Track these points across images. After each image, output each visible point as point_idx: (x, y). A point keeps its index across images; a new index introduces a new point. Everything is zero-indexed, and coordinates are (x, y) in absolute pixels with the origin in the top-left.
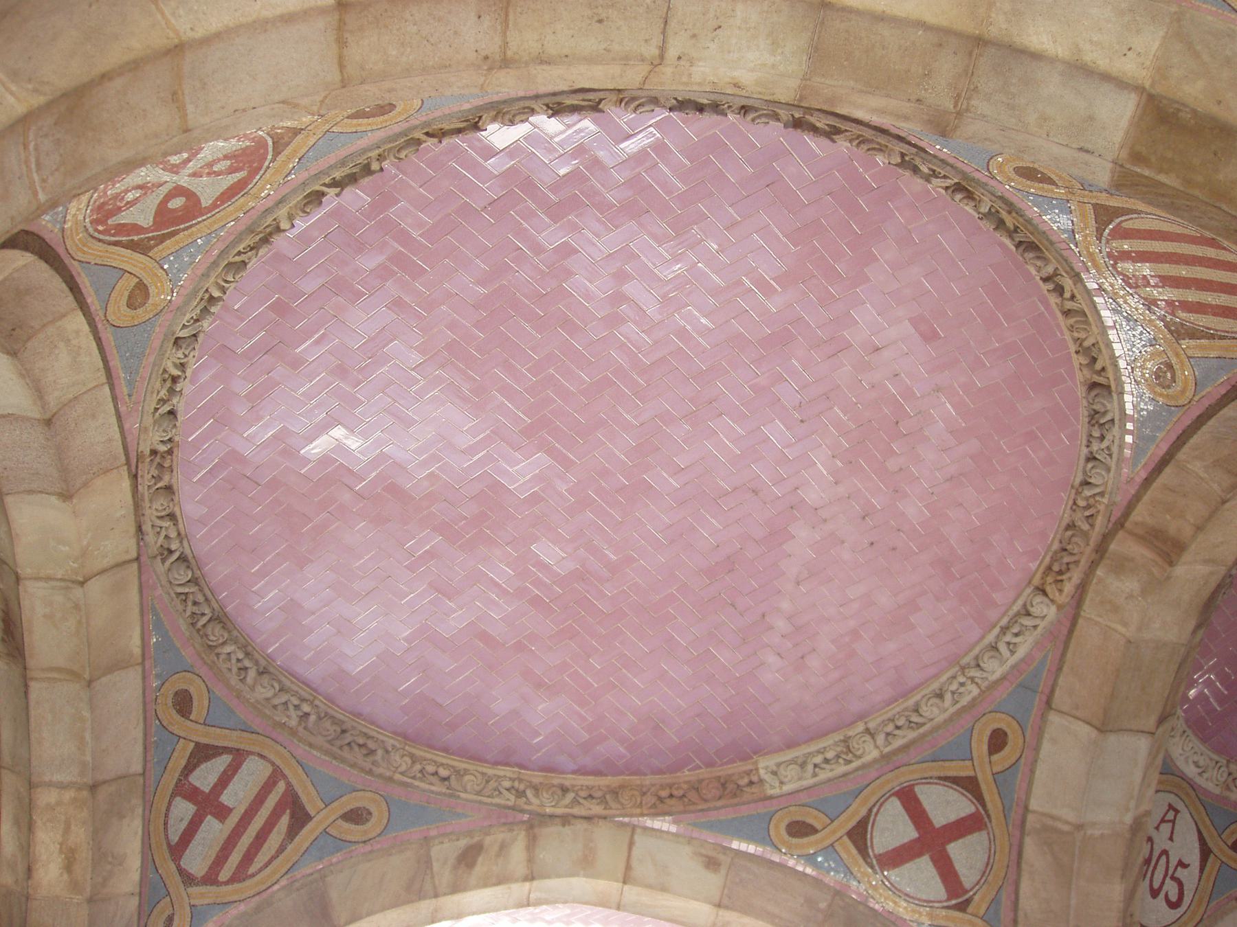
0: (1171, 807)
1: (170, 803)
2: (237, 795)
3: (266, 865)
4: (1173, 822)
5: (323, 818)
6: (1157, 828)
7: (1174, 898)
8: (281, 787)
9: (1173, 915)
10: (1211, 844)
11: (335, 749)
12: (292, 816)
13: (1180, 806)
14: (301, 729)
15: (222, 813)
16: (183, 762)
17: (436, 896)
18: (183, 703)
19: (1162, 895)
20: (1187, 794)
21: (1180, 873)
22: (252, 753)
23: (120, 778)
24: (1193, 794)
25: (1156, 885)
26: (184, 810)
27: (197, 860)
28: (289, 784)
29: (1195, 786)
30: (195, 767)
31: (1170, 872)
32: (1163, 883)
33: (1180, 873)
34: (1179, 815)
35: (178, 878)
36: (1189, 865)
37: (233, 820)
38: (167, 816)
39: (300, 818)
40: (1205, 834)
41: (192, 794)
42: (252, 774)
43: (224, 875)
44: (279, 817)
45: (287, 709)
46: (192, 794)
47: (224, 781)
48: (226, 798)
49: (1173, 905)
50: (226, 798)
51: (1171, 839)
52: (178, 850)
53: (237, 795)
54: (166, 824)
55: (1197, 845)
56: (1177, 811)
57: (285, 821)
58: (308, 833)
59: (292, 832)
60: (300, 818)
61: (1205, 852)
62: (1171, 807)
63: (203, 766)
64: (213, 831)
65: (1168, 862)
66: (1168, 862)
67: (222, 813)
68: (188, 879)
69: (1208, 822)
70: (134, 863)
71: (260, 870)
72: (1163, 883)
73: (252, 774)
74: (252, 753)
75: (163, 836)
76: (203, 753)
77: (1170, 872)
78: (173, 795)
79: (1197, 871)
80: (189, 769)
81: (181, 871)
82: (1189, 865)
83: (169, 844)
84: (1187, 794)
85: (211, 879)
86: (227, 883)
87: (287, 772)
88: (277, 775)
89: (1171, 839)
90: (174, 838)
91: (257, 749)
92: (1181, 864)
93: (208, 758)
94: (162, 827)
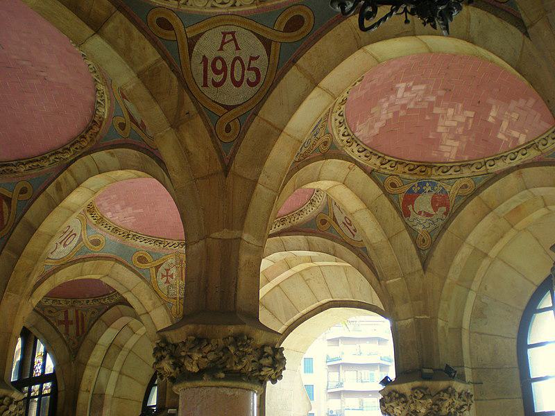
0: (224, 34)
4: (234, 39)
5: (15, 196)
6: (221, 49)
10: (269, 37)
12: (6, 201)
13: (233, 29)
17: (57, 206)
20: (232, 20)
21: (253, 64)
25: (238, 79)
31: (246, 67)
32: (243, 76)
33: (253, 64)
40: (261, 34)
49: (251, 84)
51: (238, 48)
55: (259, 42)
56: (233, 33)
58: (14, 203)
61: (267, 44)
62: (224, 34)
65: (242, 62)
66: (242, 62)
69: (260, 26)
72: (243, 76)
77: (246, 67)
79: (266, 57)
84: (232, 20)
89: (238, 48)
92: (252, 58)
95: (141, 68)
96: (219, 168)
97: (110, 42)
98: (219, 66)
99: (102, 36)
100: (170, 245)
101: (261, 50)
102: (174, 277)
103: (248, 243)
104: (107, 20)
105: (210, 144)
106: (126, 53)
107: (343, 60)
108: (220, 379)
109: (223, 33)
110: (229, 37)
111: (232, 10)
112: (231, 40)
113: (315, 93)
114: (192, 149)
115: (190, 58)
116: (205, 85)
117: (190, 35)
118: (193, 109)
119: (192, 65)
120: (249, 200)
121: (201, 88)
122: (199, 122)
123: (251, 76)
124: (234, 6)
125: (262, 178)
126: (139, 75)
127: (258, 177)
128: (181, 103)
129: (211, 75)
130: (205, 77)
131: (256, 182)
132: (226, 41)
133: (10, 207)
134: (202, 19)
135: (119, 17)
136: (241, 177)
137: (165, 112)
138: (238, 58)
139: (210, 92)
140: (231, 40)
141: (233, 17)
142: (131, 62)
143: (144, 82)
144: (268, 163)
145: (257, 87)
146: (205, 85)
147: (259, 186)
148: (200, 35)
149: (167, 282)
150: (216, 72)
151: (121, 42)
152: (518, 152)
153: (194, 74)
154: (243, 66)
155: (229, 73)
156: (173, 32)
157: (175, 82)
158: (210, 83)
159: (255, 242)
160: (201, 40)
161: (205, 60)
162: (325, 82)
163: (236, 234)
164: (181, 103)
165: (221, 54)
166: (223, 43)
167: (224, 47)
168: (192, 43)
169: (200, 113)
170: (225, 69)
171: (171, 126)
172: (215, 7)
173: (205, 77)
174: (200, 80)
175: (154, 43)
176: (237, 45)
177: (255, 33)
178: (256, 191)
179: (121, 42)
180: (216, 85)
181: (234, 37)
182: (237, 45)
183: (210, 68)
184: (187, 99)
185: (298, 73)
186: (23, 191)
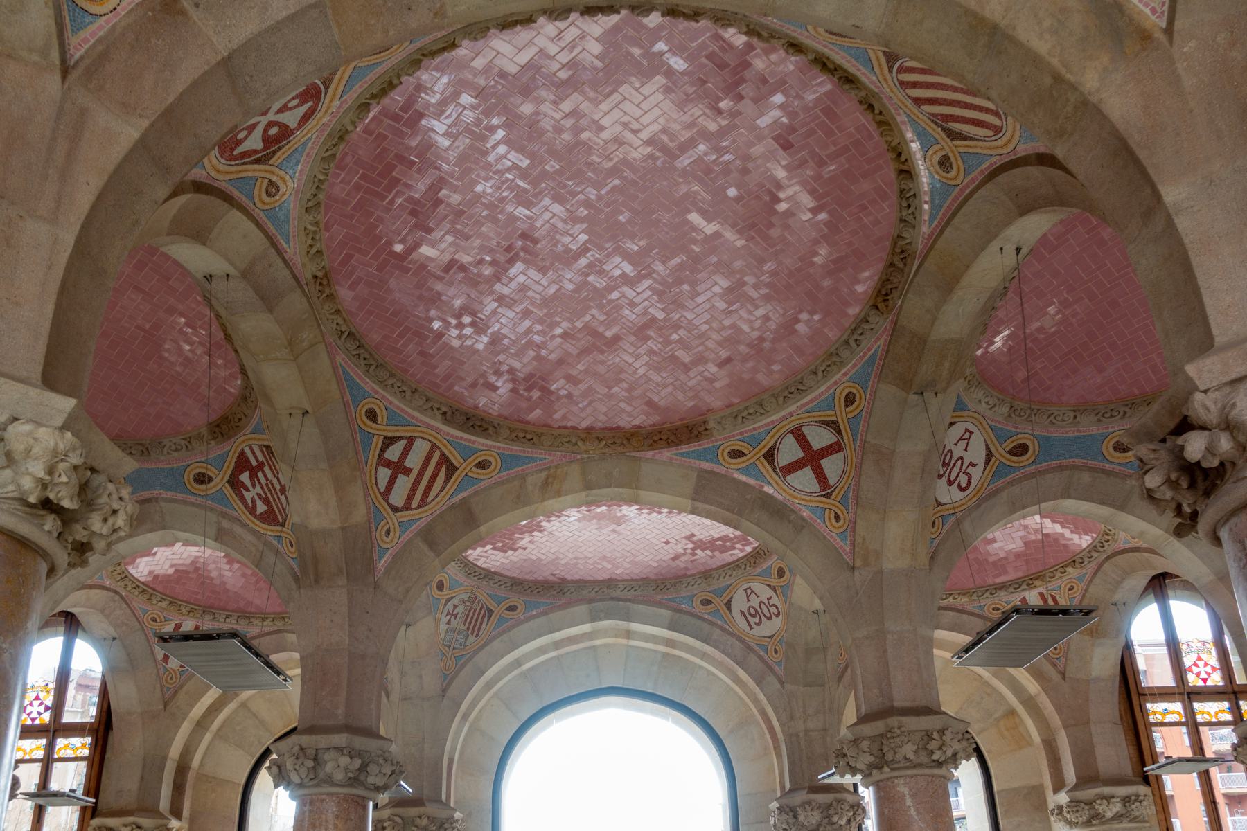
1: (376, 469)
2: (414, 461)
3: (436, 497)
7: (964, 485)
8: (437, 455)
9: (960, 495)
12: (447, 469)
15: (407, 471)
19: (956, 484)
21: (970, 470)
22: (415, 437)
25: (952, 478)
26: (384, 474)
27: (398, 498)
32: (958, 476)
33: (970, 470)
35: (389, 509)
37: (414, 475)
39: (451, 470)
41: (388, 464)
43: (415, 504)
44: (439, 470)
45: (433, 410)
46: (388, 464)
48: (408, 463)
49: (962, 489)
50: (408, 463)
53: (414, 461)
59: (448, 477)
60: (451, 470)
64: (403, 483)
65: (962, 463)
66: (962, 463)
67: (407, 471)
68: (395, 509)
71: (433, 500)
72: (958, 476)
76: (389, 441)
78: (378, 465)
80: (383, 450)
83: (380, 493)
85: (407, 507)
87: (438, 444)
88: (434, 447)
89: (966, 450)
90: (382, 490)
91: (421, 435)
93: (392, 443)
100: (476, 574)
102: (458, 618)
123: (963, 480)
133: (448, 477)
145: (966, 493)
149: (449, 623)
152: (1056, 570)
154: (961, 467)
176: (967, 447)
182: (967, 447)
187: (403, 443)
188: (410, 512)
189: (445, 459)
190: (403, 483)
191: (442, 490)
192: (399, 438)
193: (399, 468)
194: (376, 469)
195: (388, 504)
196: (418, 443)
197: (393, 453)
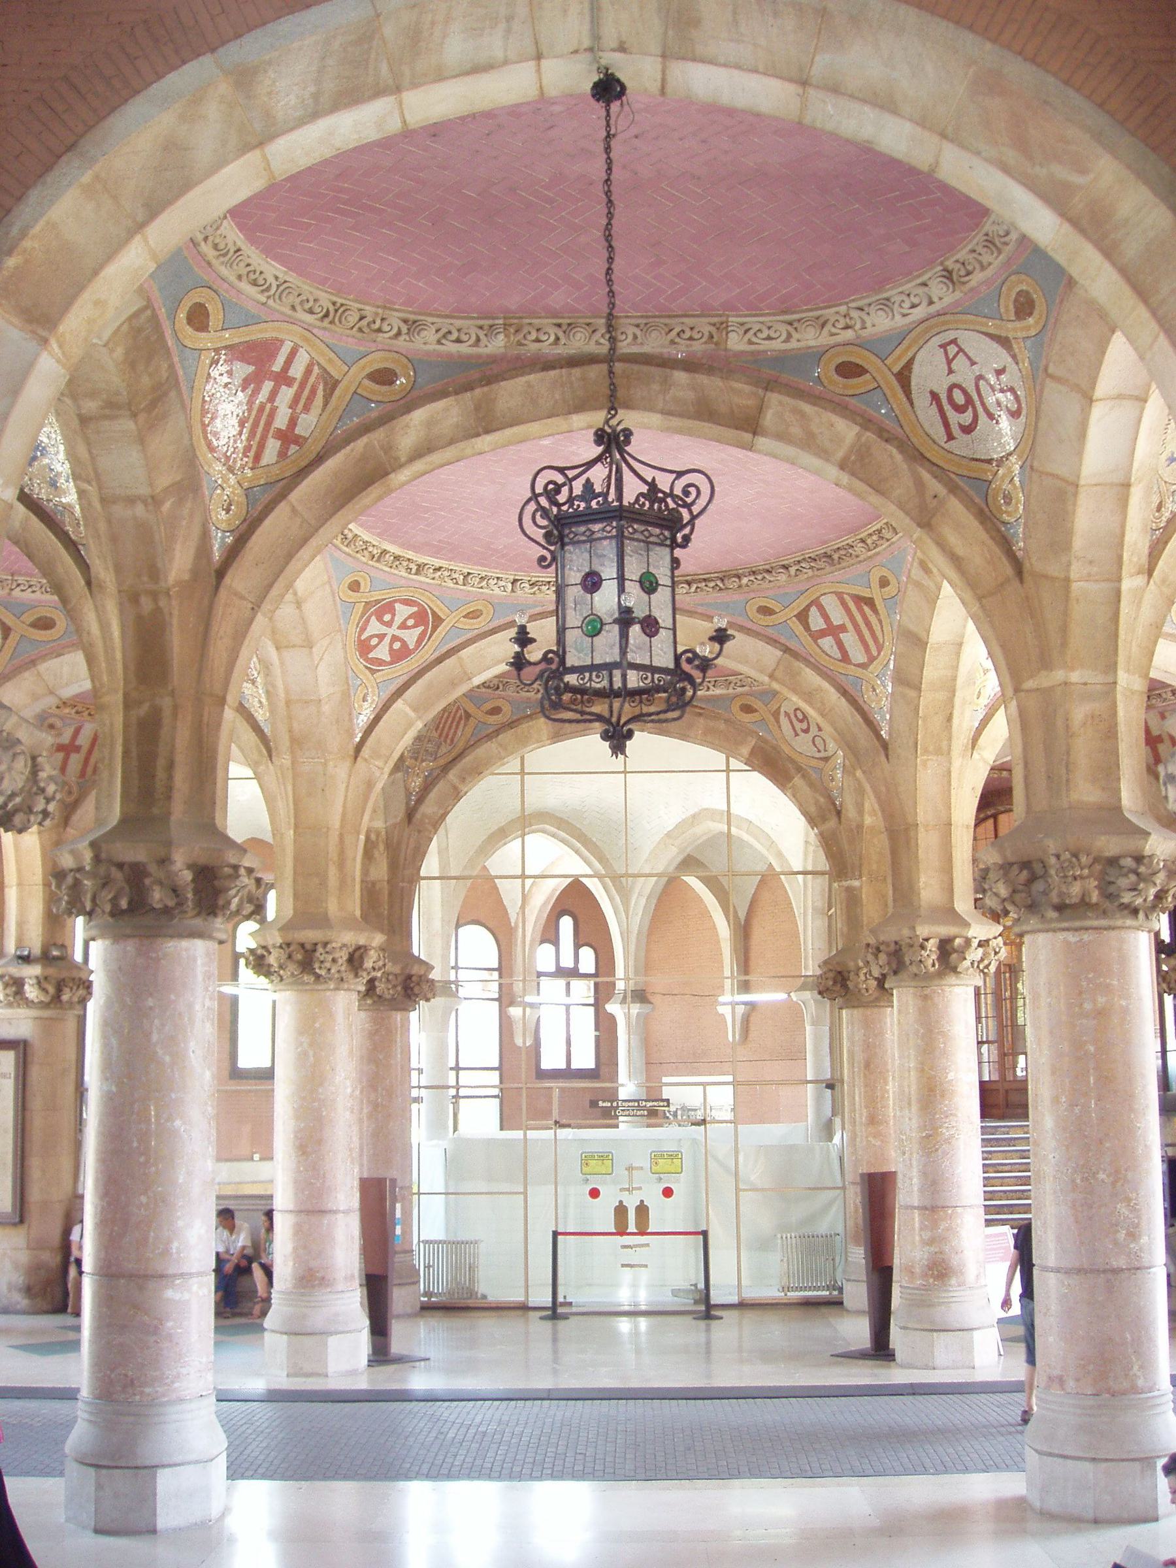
0: (943, 346)
1: (818, 645)
2: (838, 617)
4: (961, 350)
5: (876, 593)
6: (951, 371)
11: (838, 566)
13: (951, 335)
14: (816, 573)
15: (842, 628)
16: (801, 628)
18: (765, 611)
20: (944, 323)
22: (819, 597)
23: (778, 663)
24: (948, 317)
26: (827, 642)
28: (848, 594)
29: (941, 312)
30: (808, 624)
34: (959, 342)
35: (860, 670)
36: (1005, 367)
37: (849, 626)
38: (823, 652)
39: (870, 602)
41: (823, 633)
42: (831, 604)
43: (875, 653)
46: (823, 633)
47: (826, 617)
52: (845, 658)
54: (827, 654)
55: (995, 345)
56: (954, 342)
57: (866, 609)
62: (943, 346)
63: (810, 620)
70: (826, 685)
73: (831, 604)
74: (819, 597)
75: (832, 660)
76: (803, 617)
80: (807, 627)
81: (859, 665)
82: (1005, 367)
83: (840, 661)
86: (879, 654)
88: (840, 596)
89: (973, 363)
90: (839, 656)
91: (819, 594)
92: (999, 372)
93: (807, 617)
94: (827, 657)
95: (840, 454)
96: (1009, 571)
97: (781, 437)
98: (959, 398)
99: (764, 434)
101: (1003, 358)
103: (1085, 684)
104: (760, 409)
105: (983, 535)
106: (809, 442)
107: (1103, 353)
108: (1051, 920)
109: (941, 346)
110: (952, 350)
111: (933, 309)
112: (958, 353)
113: (1097, 411)
114: (960, 551)
115: (912, 404)
116: (950, 437)
117: (896, 369)
118: (941, 490)
119: (918, 412)
120: (1066, 613)
121: (947, 446)
122: (955, 505)
124: (931, 303)
125: (1076, 570)
126: (842, 466)
127: (1068, 571)
128: (920, 485)
129: (953, 417)
130: (946, 425)
131: (1067, 580)
132: (951, 357)
134: (902, 336)
135: (774, 398)
136: (1046, 577)
137: (901, 506)
138: (980, 377)
139: (962, 445)
140: (958, 353)
141: (942, 318)
142: (823, 454)
143: (853, 474)
144: (1078, 543)
145: (1023, 419)
146: (950, 437)
147: (1075, 586)
148: (911, 362)
150: (960, 409)
151: (796, 430)
153: (926, 426)
155: (978, 403)
156: (867, 377)
157: (899, 458)
158: (956, 431)
159: (1100, 678)
160: (916, 367)
161: (935, 396)
162: (1099, 392)
163: (1059, 675)
164: (920, 485)
165: (953, 379)
166: (949, 362)
167: (954, 366)
168: (904, 378)
169: (953, 489)
170: (969, 401)
171: (919, 525)
172: (907, 315)
173: (946, 425)
174: (939, 433)
175: (842, 408)
177: (983, 333)
178: (1073, 595)
179: (796, 430)
180: (968, 430)
181: (958, 346)
183: (947, 407)
184: (926, 476)
185: (1060, 387)
186: (884, 583)
187: (813, 609)
188: (877, 661)
189: (858, 599)
190: (849, 639)
191: (880, 621)
192: (807, 609)
193: (833, 631)
194: (818, 645)
195: (855, 665)
196: (824, 601)
197: (816, 622)
